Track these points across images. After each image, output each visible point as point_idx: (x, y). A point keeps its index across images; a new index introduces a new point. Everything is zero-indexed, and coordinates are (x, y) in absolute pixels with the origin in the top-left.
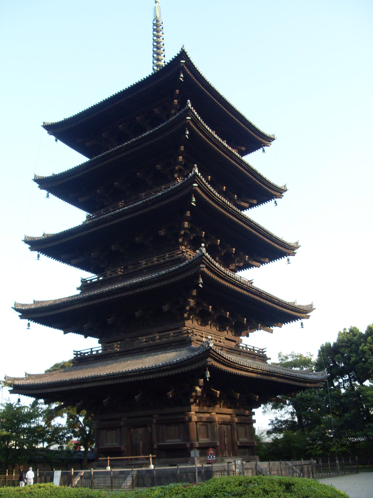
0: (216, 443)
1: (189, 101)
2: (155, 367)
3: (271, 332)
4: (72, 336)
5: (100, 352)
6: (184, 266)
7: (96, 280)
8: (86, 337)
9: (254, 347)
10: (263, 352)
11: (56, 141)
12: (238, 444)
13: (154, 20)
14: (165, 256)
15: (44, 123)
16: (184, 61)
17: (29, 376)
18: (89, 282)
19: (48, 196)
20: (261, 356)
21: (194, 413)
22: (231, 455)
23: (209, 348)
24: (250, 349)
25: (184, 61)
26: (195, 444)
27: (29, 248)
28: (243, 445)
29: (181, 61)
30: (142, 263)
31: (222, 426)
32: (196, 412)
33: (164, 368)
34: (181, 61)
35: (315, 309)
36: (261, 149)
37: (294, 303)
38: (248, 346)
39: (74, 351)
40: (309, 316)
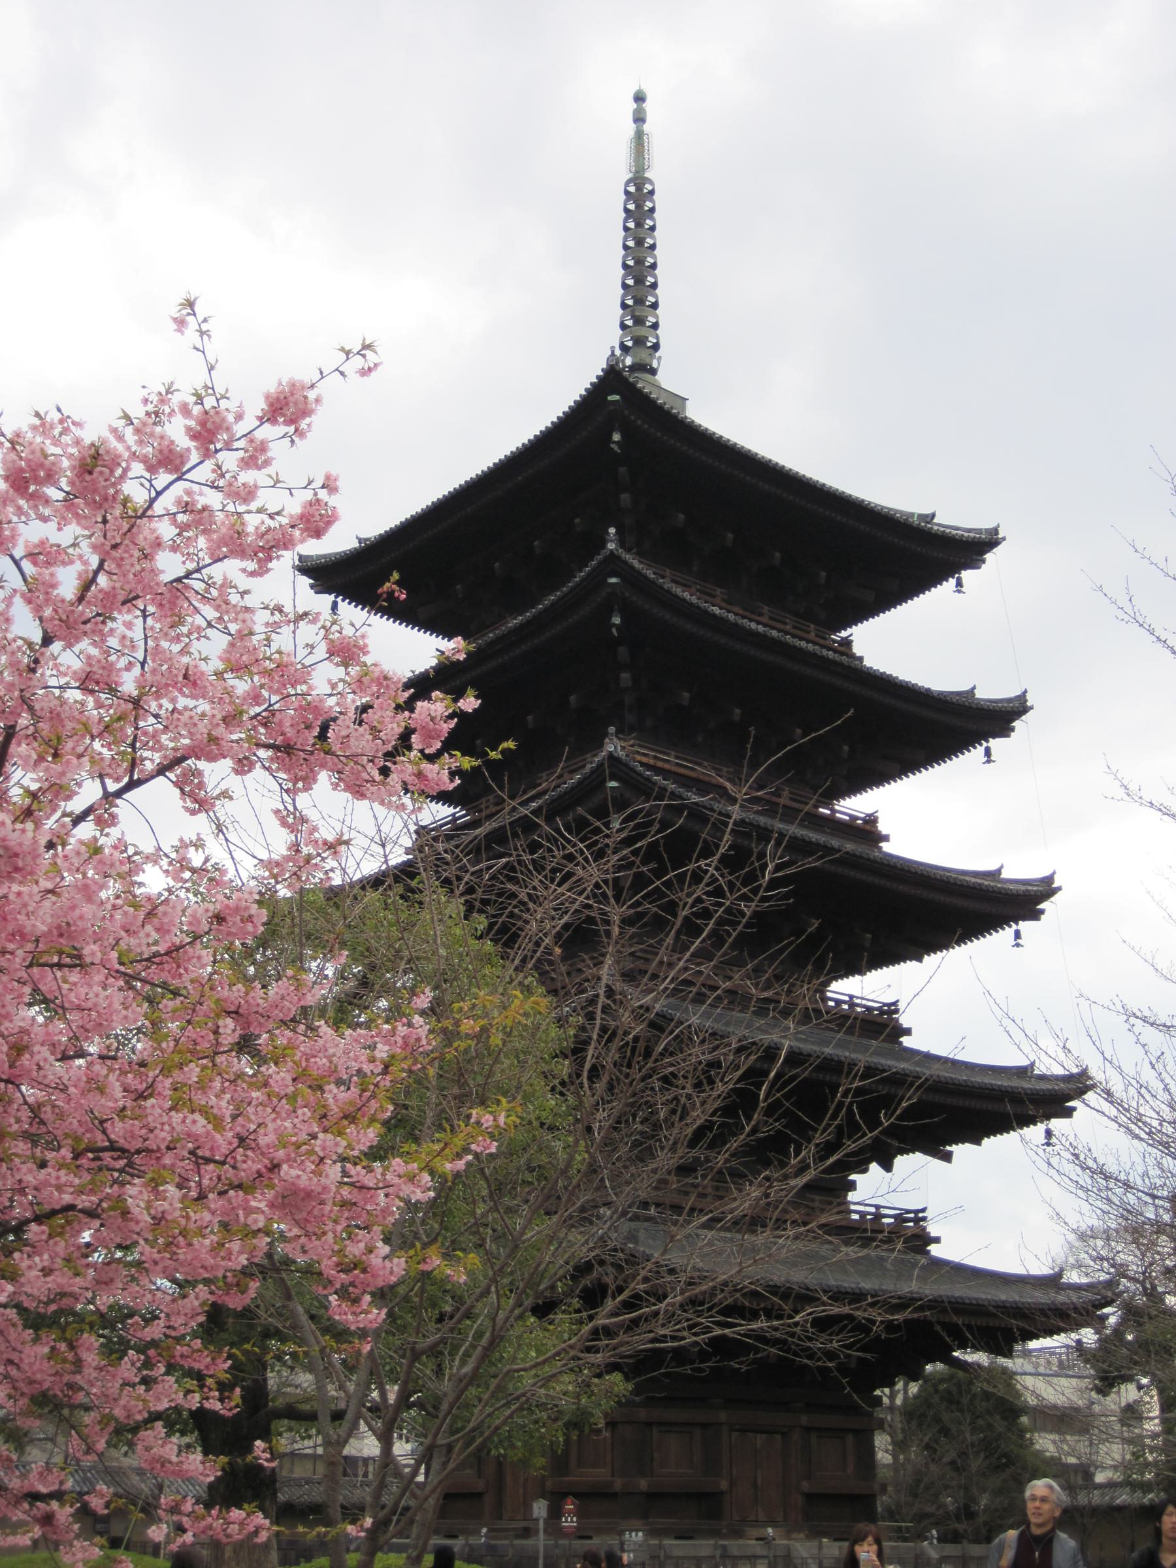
1: (612, 530)
3: (947, 1157)
10: (917, 1220)
13: (627, 183)
15: (301, 557)
16: (617, 397)
25: (617, 397)
29: (609, 398)
31: (750, 1434)
34: (609, 398)
36: (952, 582)
40: (1074, 1109)
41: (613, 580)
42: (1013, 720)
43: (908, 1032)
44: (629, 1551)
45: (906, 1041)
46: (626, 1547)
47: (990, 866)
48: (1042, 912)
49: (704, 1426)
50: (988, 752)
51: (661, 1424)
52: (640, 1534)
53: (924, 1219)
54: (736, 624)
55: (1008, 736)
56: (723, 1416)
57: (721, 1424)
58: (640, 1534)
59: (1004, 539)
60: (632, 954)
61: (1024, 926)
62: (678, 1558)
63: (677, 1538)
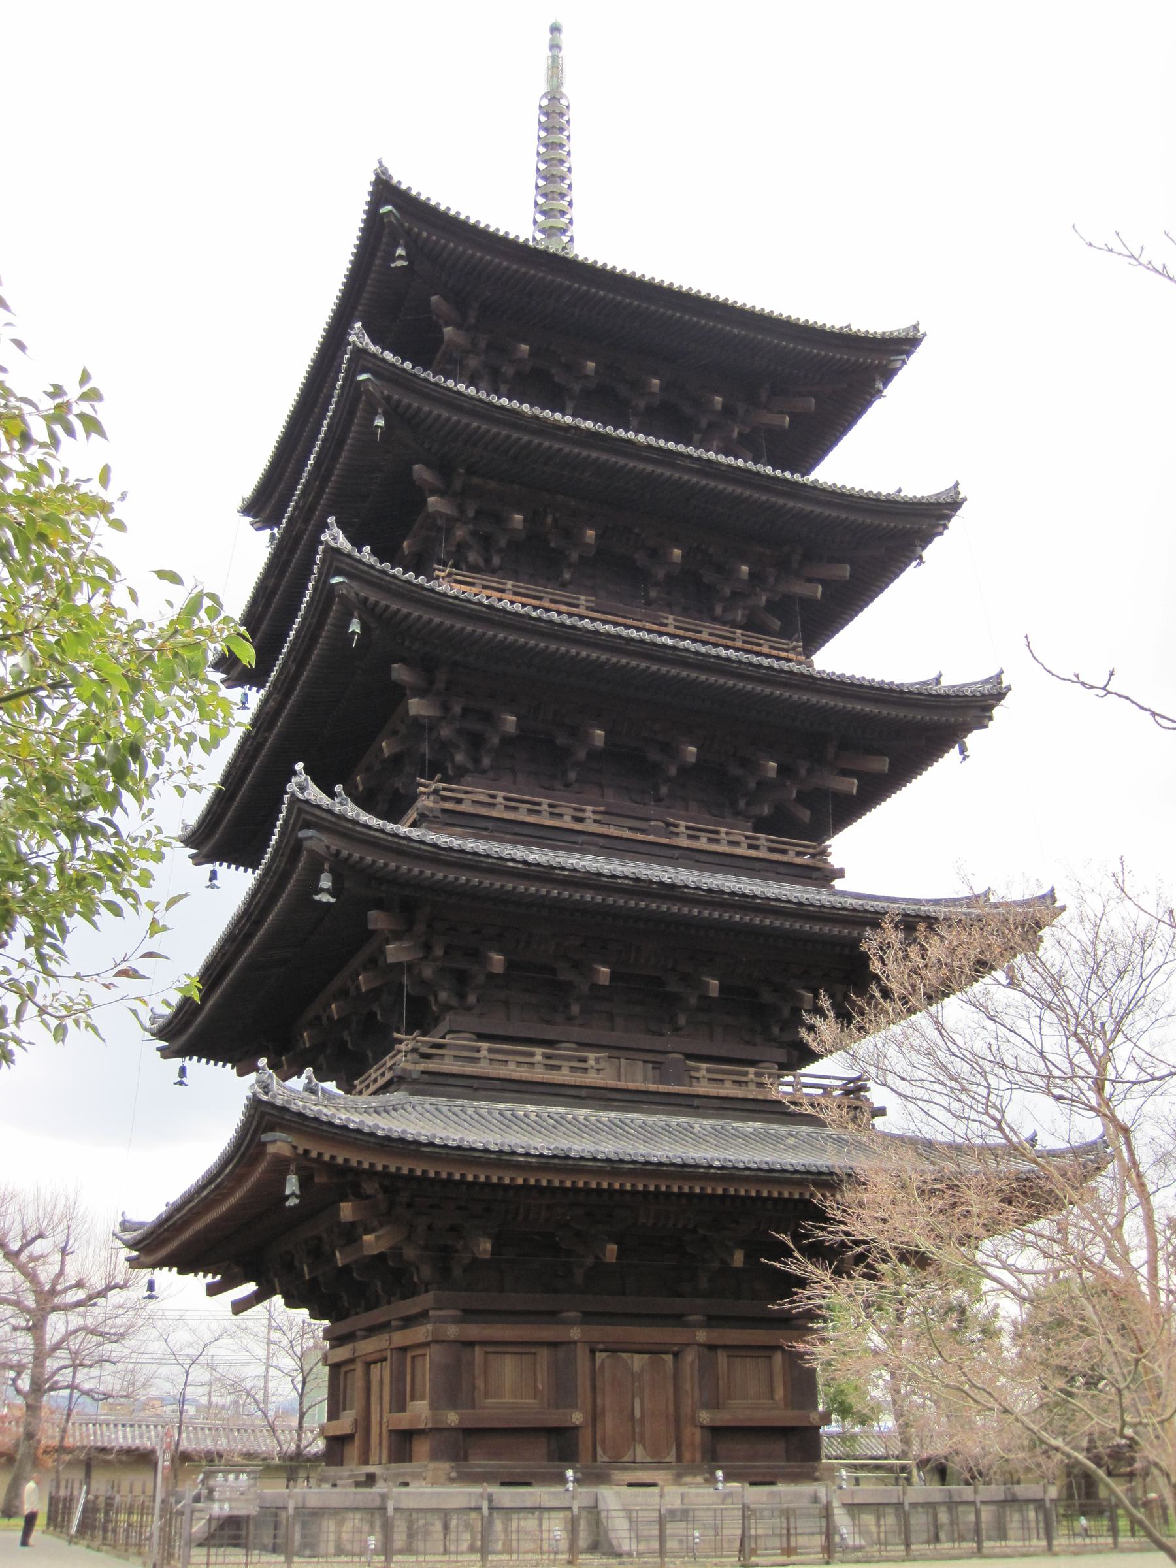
16: (389, 208)
25: (389, 208)
27: (192, 857)
31: (624, 1355)
34: (382, 211)
35: (1063, 908)
41: (363, 377)
43: (840, 873)
44: (221, 1501)
45: (838, 884)
46: (216, 1495)
47: (929, 676)
49: (554, 1345)
51: (483, 1343)
53: (864, 1088)
56: (575, 1333)
57: (575, 1343)
58: (244, 1477)
59: (925, 335)
60: (436, 792)
62: (411, 1510)
63: (503, 1484)
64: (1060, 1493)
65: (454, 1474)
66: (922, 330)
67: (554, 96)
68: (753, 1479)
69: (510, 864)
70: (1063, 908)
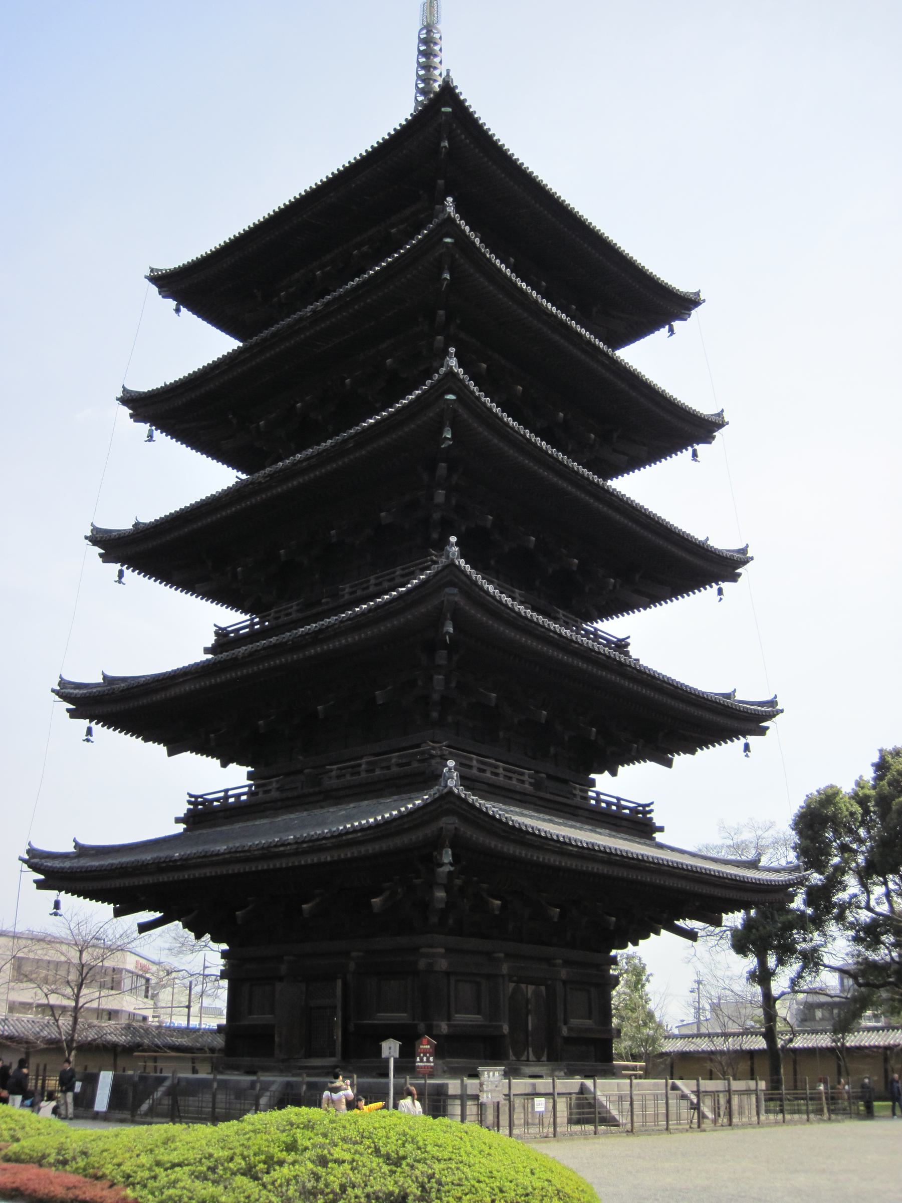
0: (501, 1027)
1: (450, 199)
2: (329, 835)
3: (668, 764)
4: (188, 758)
5: (244, 798)
6: (409, 592)
7: (247, 630)
8: (224, 765)
9: (619, 799)
10: (645, 813)
11: (178, 310)
12: (565, 1031)
14: (394, 572)
15: (152, 270)
16: (450, 110)
17: (82, 851)
18: (232, 635)
19: (150, 437)
20: (639, 823)
21: (442, 950)
22: (544, 1058)
23: (446, 790)
24: (609, 804)
25: (450, 110)
26: (439, 1026)
27: (101, 555)
28: (574, 1035)
29: (443, 109)
30: (344, 589)
31: (523, 986)
32: (447, 950)
33: (350, 836)
34: (443, 109)
35: (782, 711)
36: (667, 327)
37: (728, 696)
38: (602, 797)
39: (191, 796)
40: (767, 728)
41: (448, 240)
42: (715, 431)
44: (487, 1092)
48: (739, 575)
50: (695, 454)
52: (497, 1074)
53: (651, 811)
54: (536, 302)
55: (710, 443)
61: (726, 586)
64: (767, 1086)
65: (445, 1068)
66: (702, 298)
67: (429, 28)
68: (588, 1074)
69: (551, 634)
70: (782, 711)
